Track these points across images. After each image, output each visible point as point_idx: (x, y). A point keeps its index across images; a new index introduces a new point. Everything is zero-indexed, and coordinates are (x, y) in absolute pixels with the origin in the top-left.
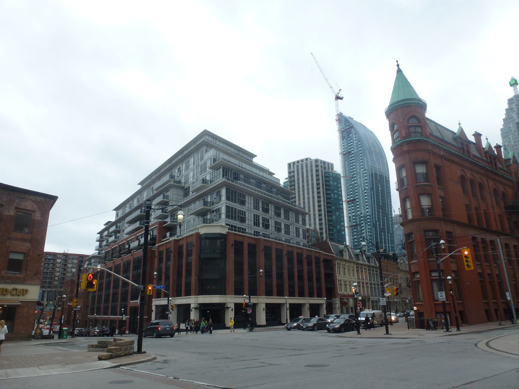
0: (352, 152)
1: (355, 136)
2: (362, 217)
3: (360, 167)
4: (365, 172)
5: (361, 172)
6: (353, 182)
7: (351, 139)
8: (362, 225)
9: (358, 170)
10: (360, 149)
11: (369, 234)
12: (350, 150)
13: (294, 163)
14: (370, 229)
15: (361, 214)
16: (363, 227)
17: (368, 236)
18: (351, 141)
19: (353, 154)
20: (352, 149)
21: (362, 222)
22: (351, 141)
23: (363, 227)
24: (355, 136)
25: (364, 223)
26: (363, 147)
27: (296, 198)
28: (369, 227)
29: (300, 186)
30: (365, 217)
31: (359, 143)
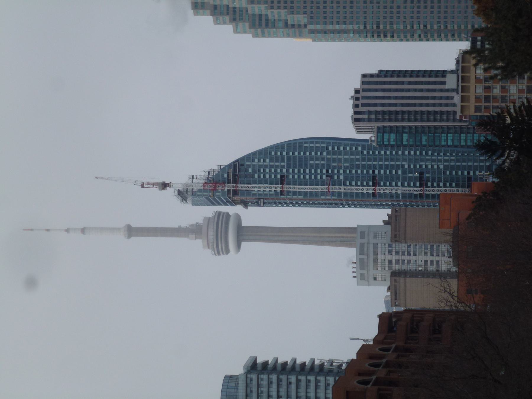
0: (284, 171)
1: (256, 160)
2: (409, 166)
3: (317, 159)
4: (330, 148)
5: (328, 157)
6: (342, 177)
7: (259, 171)
8: (424, 167)
9: (323, 162)
10: (285, 153)
11: (441, 156)
12: (279, 176)
13: (356, 113)
14: (433, 152)
15: (403, 166)
16: (427, 166)
17: (446, 158)
18: (262, 170)
19: (287, 171)
20: (279, 171)
21: (418, 166)
22: (262, 170)
23: (427, 166)
24: (256, 160)
25: (421, 163)
27: (410, 110)
28: (430, 153)
29: (394, 103)
30: (410, 161)
31: (273, 153)
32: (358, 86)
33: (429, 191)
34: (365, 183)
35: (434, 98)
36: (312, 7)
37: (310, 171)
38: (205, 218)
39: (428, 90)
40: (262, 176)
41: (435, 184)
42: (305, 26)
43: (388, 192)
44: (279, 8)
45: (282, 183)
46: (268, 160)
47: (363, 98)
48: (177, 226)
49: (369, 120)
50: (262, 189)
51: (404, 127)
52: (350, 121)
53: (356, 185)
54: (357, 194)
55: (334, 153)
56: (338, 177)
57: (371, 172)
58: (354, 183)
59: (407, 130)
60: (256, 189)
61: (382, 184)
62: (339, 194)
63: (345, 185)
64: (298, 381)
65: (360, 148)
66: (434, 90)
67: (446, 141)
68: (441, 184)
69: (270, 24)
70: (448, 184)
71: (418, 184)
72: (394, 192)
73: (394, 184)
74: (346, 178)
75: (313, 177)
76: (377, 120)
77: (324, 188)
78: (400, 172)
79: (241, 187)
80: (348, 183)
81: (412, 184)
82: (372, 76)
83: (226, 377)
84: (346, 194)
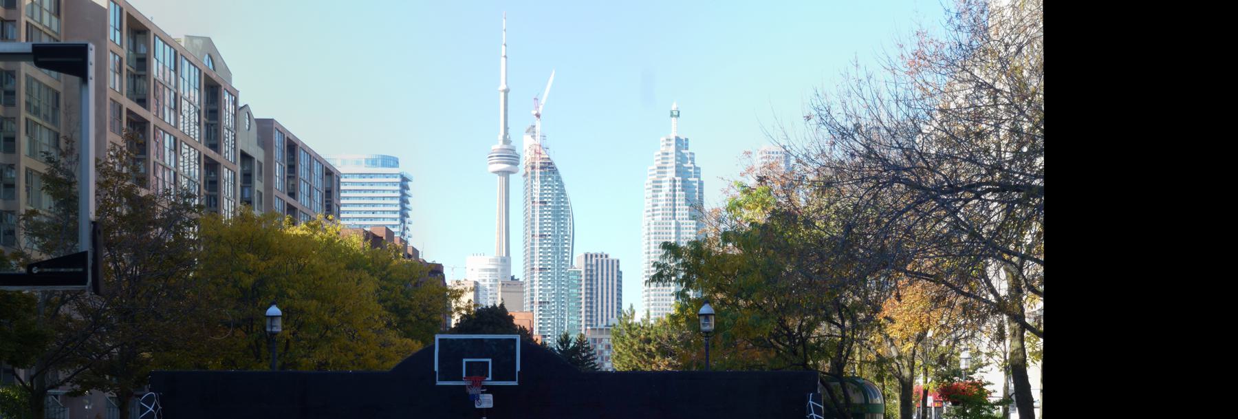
0: (550, 204)
1: (557, 184)
4: (566, 237)
6: (545, 246)
7: (549, 186)
12: (545, 200)
15: (554, 289)
18: (550, 188)
19: (549, 206)
20: (550, 200)
22: (550, 188)
24: (557, 184)
26: (567, 203)
31: (563, 196)
32: (611, 257)
33: (536, 308)
34: (541, 263)
35: (602, 311)
36: (666, 224)
37: (550, 223)
38: (515, 147)
39: (607, 307)
40: (546, 188)
41: (541, 312)
42: (653, 219)
43: (535, 279)
44: (667, 200)
45: (540, 202)
46: (557, 192)
47: (602, 261)
48: (509, 126)
49: (586, 265)
50: (536, 188)
51: (581, 290)
52: (586, 252)
53: (540, 256)
54: (533, 257)
55: (562, 241)
56: (545, 243)
57: (549, 267)
58: (541, 254)
59: (579, 292)
60: (536, 183)
61: (541, 275)
62: (533, 244)
63: (540, 248)
64: (395, 212)
65: (566, 259)
66: (607, 311)
67: (572, 319)
68: (541, 317)
69: (654, 194)
70: (541, 321)
71: (541, 300)
72: (535, 283)
73: (541, 283)
74: (545, 249)
75: (545, 225)
76: (586, 270)
77: (537, 233)
78: (549, 287)
79: (538, 171)
80: (541, 250)
81: (541, 296)
82: (618, 267)
83: (397, 159)
84: (533, 249)
